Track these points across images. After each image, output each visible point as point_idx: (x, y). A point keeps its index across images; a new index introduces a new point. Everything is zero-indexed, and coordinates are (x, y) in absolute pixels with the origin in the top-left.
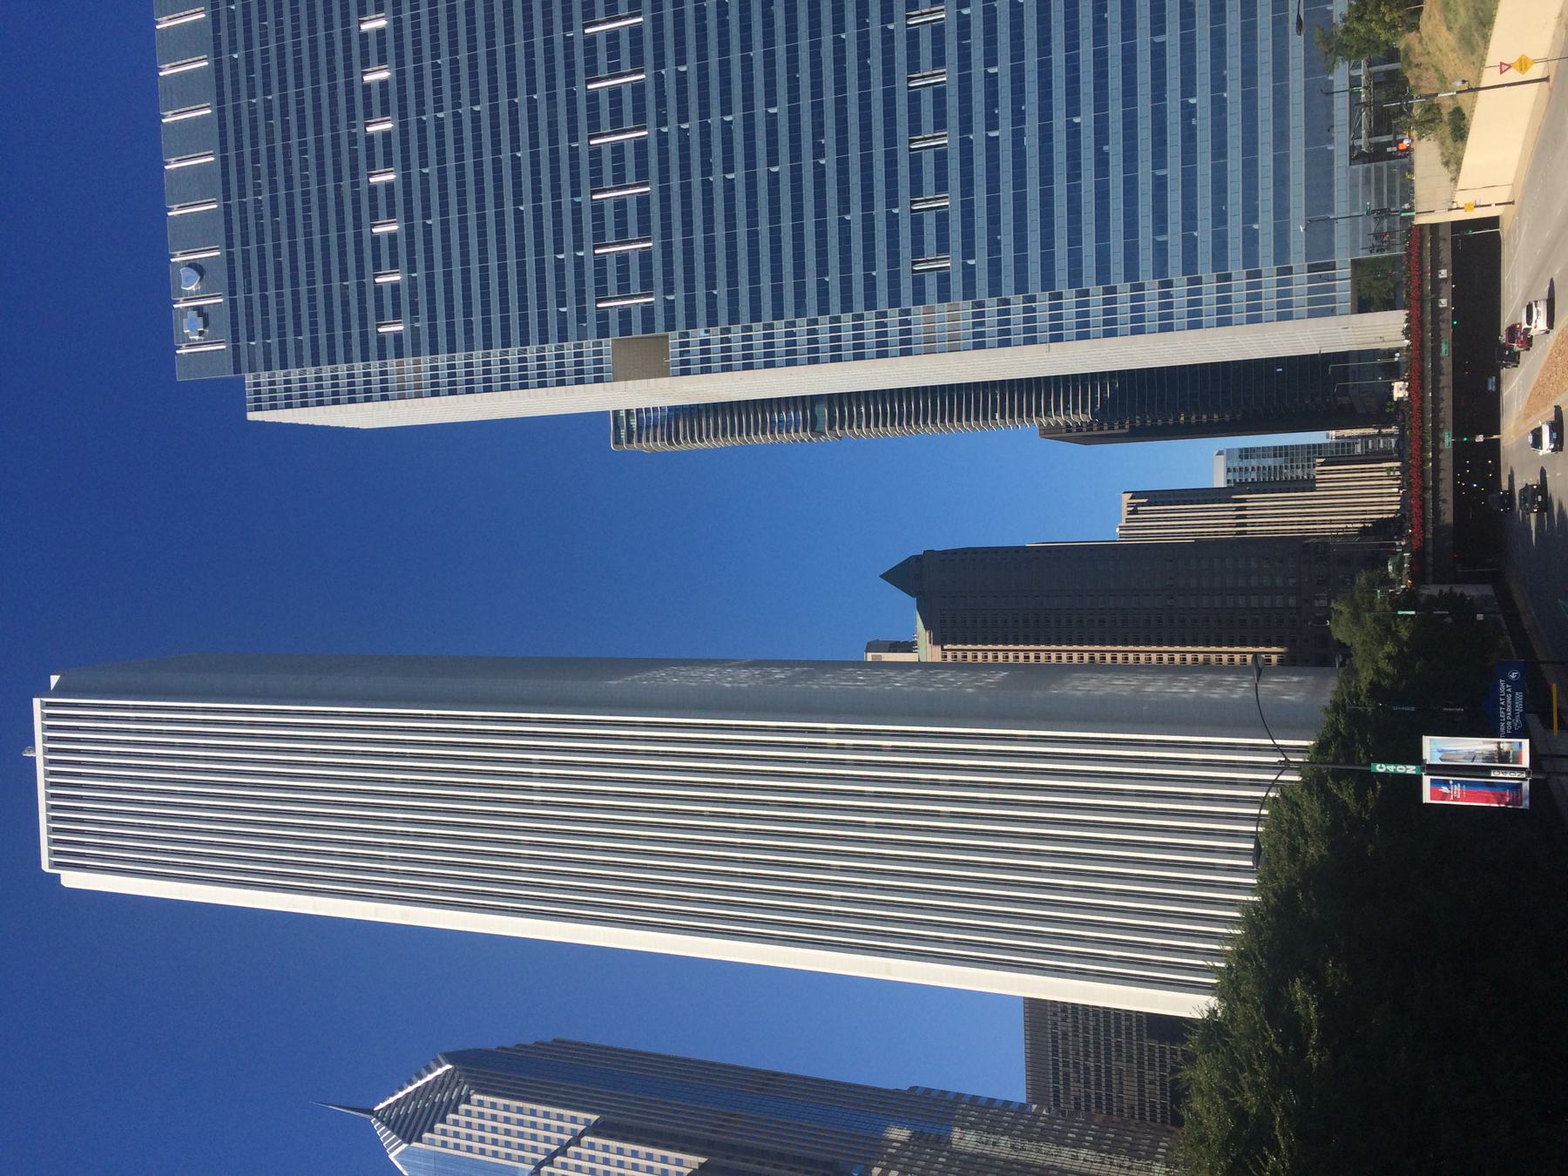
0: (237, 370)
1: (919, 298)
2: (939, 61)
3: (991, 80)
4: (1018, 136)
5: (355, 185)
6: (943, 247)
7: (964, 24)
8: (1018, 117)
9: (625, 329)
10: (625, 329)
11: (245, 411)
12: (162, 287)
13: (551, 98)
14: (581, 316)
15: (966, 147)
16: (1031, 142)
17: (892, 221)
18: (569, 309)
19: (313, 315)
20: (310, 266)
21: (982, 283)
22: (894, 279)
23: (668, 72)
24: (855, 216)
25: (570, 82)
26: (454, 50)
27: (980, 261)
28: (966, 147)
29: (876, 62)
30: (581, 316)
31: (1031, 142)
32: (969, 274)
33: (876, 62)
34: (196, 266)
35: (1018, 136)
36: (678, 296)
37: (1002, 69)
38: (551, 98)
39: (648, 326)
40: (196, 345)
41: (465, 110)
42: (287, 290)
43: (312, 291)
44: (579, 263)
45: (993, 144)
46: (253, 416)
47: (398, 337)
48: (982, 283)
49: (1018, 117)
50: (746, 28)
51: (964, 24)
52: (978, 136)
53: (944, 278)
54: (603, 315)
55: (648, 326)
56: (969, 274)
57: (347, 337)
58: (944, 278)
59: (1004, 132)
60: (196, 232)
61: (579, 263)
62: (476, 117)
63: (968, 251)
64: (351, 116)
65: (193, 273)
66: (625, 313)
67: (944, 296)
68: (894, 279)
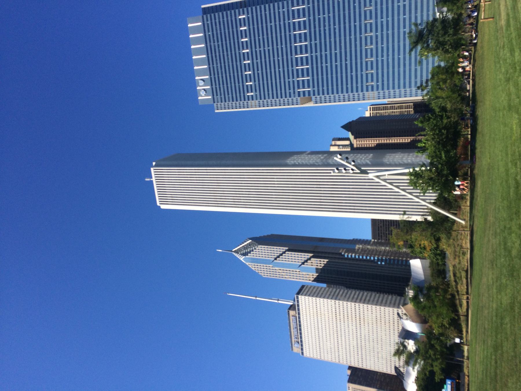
0: (214, 102)
1: (367, 90)
2: (371, 44)
3: (382, 48)
4: (388, 59)
5: (241, 63)
6: (372, 81)
7: (377, 37)
8: (388, 55)
9: (304, 95)
10: (304, 95)
11: (214, 110)
12: (195, 84)
13: (286, 47)
14: (294, 93)
15: (377, 61)
16: (390, 60)
17: (362, 75)
18: (292, 91)
19: (232, 91)
20: (231, 80)
21: (380, 87)
22: (362, 86)
23: (313, 42)
24: (354, 73)
25: (291, 43)
26: (263, 35)
27: (380, 83)
28: (377, 61)
29: (358, 43)
30: (294, 93)
31: (390, 60)
32: (378, 86)
33: (358, 43)
34: (203, 80)
35: (388, 59)
36: (316, 89)
37: (385, 45)
38: (286, 47)
39: (309, 94)
40: (203, 97)
41: (266, 49)
42: (225, 86)
43: (231, 86)
44: (293, 81)
45: (382, 60)
46: (216, 111)
47: (252, 96)
48: (380, 87)
49: (388, 55)
50: (330, 35)
51: (377, 37)
52: (380, 59)
53: (372, 87)
54: (299, 92)
55: (309, 94)
56: (378, 86)
57: (240, 96)
58: (372, 86)
59: (385, 58)
60: (201, 72)
61: (293, 81)
62: (269, 50)
63: (377, 81)
64: (239, 49)
65: (202, 81)
66: (304, 92)
67: (372, 90)
68: (362, 86)
